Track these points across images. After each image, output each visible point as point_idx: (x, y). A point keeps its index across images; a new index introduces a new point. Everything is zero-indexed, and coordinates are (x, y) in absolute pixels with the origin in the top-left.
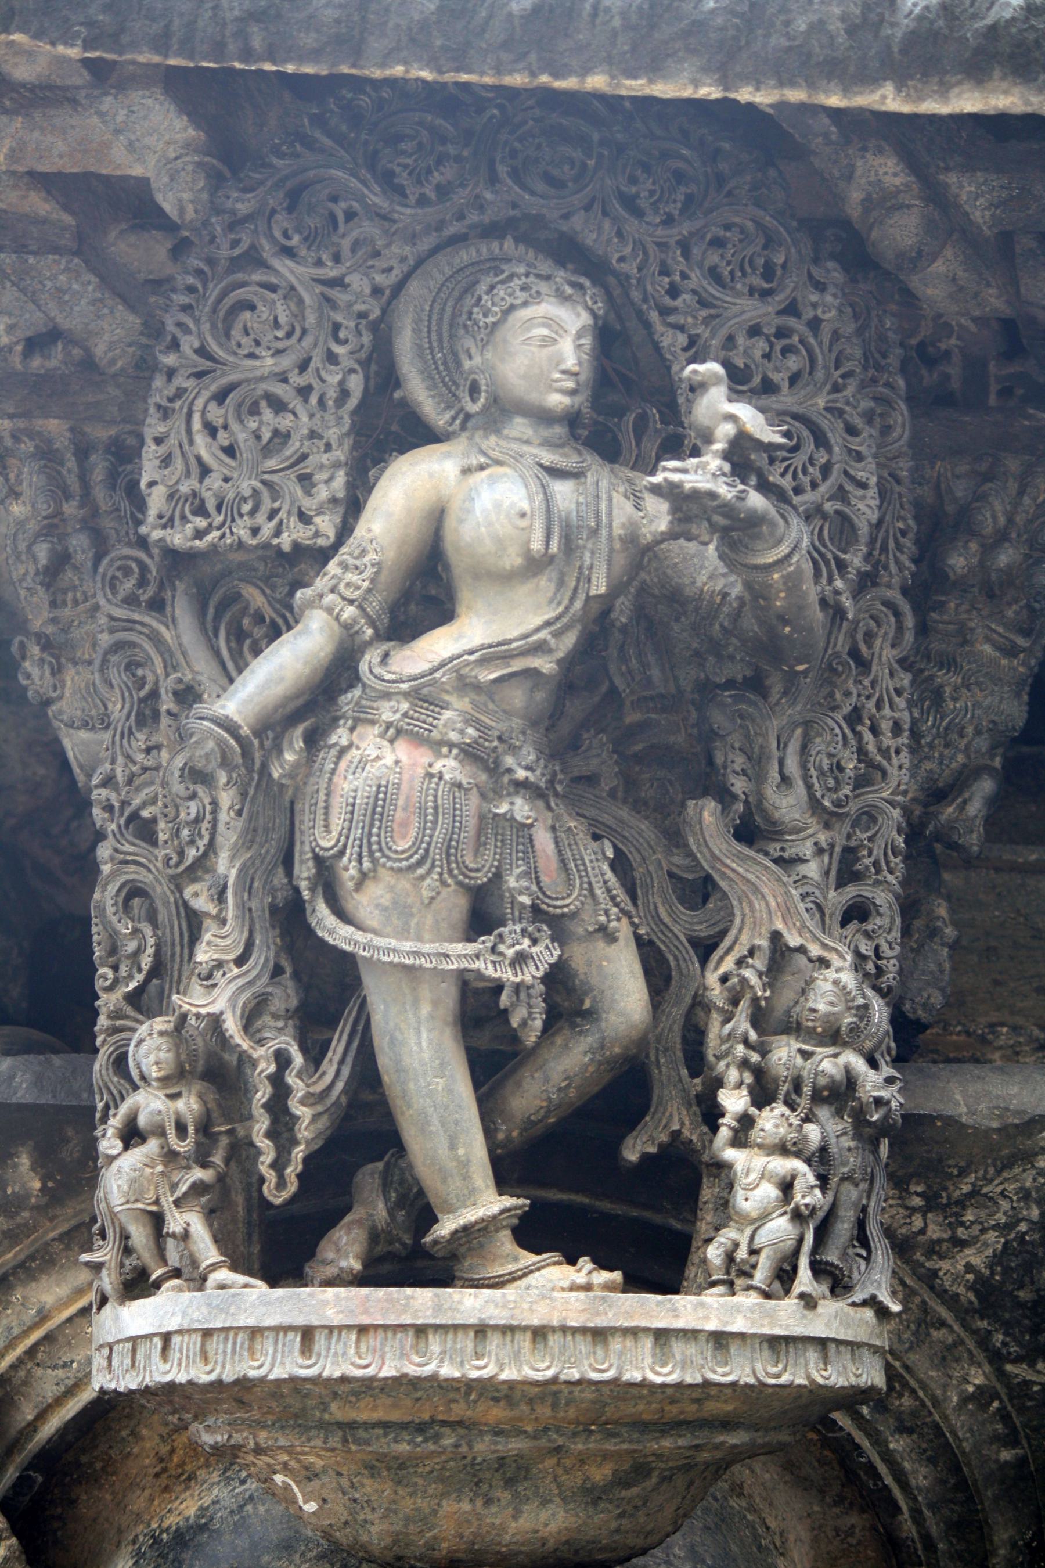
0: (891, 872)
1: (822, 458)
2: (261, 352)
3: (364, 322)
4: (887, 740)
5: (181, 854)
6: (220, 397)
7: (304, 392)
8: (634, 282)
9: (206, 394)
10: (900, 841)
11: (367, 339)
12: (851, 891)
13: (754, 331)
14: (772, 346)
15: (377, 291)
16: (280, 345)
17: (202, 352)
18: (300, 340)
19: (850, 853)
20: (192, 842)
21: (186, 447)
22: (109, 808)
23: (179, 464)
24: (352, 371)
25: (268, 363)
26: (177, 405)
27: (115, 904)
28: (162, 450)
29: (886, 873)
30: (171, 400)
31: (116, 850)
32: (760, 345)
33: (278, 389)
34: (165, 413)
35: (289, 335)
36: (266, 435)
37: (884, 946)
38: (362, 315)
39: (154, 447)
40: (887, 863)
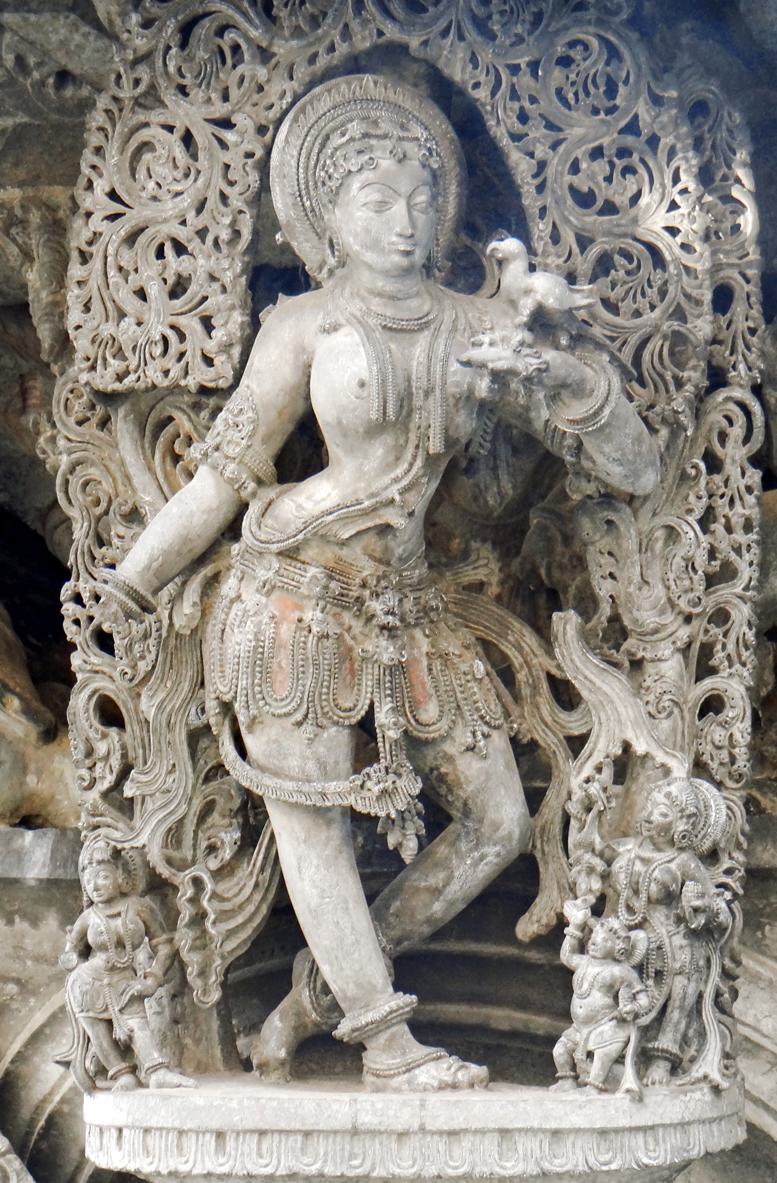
0: (744, 665)
1: (658, 277)
2: (160, 193)
3: (250, 161)
4: (740, 537)
5: (134, 667)
6: (131, 239)
7: (202, 233)
8: (489, 108)
9: (116, 239)
10: (751, 636)
11: (253, 178)
12: (708, 683)
13: (597, 153)
14: (612, 165)
15: (261, 130)
16: (178, 188)
17: (113, 195)
18: (196, 180)
19: (707, 650)
20: (143, 658)
21: (103, 290)
22: (77, 622)
23: (96, 306)
24: (241, 212)
25: (170, 207)
26: (93, 249)
27: (87, 711)
28: (83, 293)
29: (738, 666)
30: (90, 243)
31: (85, 662)
32: (600, 167)
33: (182, 234)
34: (85, 258)
35: (187, 176)
36: (171, 280)
37: (737, 736)
38: (250, 155)
39: (76, 291)
40: (739, 656)
